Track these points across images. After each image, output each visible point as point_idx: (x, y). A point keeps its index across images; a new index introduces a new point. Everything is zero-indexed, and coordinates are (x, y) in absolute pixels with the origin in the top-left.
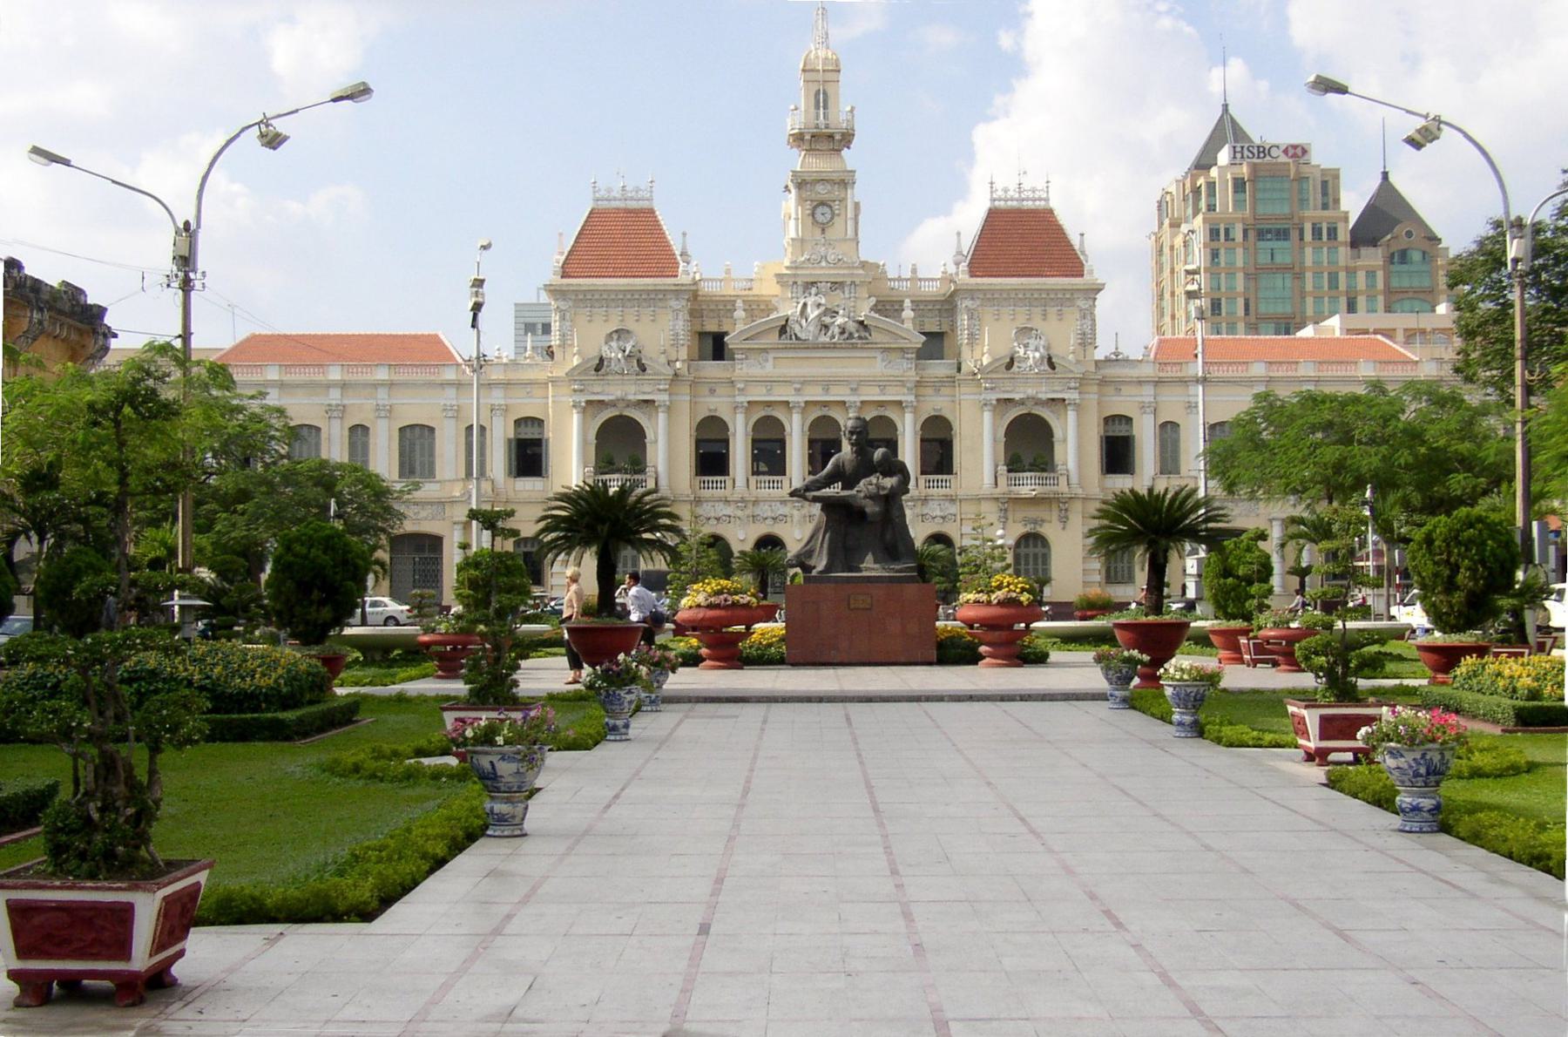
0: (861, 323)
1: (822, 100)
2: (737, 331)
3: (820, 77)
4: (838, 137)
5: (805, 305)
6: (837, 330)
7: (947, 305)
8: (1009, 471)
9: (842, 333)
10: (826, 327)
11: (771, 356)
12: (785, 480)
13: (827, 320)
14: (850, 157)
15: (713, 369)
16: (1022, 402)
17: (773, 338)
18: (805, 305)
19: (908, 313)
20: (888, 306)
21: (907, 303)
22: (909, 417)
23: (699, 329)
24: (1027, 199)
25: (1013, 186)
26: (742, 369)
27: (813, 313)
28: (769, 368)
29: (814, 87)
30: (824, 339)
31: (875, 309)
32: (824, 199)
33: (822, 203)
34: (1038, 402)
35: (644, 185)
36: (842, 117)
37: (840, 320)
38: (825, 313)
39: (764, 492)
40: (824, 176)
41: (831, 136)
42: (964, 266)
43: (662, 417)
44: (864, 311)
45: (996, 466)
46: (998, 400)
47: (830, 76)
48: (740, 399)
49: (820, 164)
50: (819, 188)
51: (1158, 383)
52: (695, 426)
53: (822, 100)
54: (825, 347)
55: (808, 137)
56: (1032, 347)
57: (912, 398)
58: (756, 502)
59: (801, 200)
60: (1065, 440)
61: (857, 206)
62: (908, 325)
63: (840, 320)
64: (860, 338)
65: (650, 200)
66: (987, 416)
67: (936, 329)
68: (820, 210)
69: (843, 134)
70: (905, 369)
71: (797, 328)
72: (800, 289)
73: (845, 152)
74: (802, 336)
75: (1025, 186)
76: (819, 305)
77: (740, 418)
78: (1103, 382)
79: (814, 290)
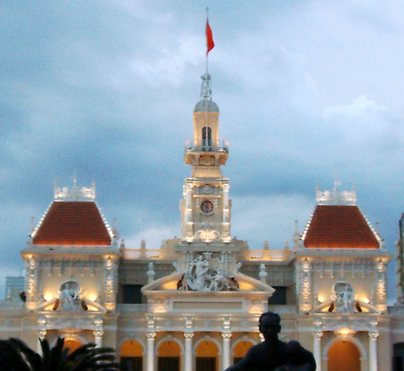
0: (233, 279)
5: (195, 267)
7: (290, 266)
13: (209, 277)
18: (195, 267)
23: (123, 283)
27: (200, 272)
38: (209, 272)
54: (207, 295)
56: (345, 297)
60: (368, 360)
63: (218, 277)
67: (282, 284)
72: (192, 257)
73: (222, 167)
76: (204, 267)
79: (201, 257)
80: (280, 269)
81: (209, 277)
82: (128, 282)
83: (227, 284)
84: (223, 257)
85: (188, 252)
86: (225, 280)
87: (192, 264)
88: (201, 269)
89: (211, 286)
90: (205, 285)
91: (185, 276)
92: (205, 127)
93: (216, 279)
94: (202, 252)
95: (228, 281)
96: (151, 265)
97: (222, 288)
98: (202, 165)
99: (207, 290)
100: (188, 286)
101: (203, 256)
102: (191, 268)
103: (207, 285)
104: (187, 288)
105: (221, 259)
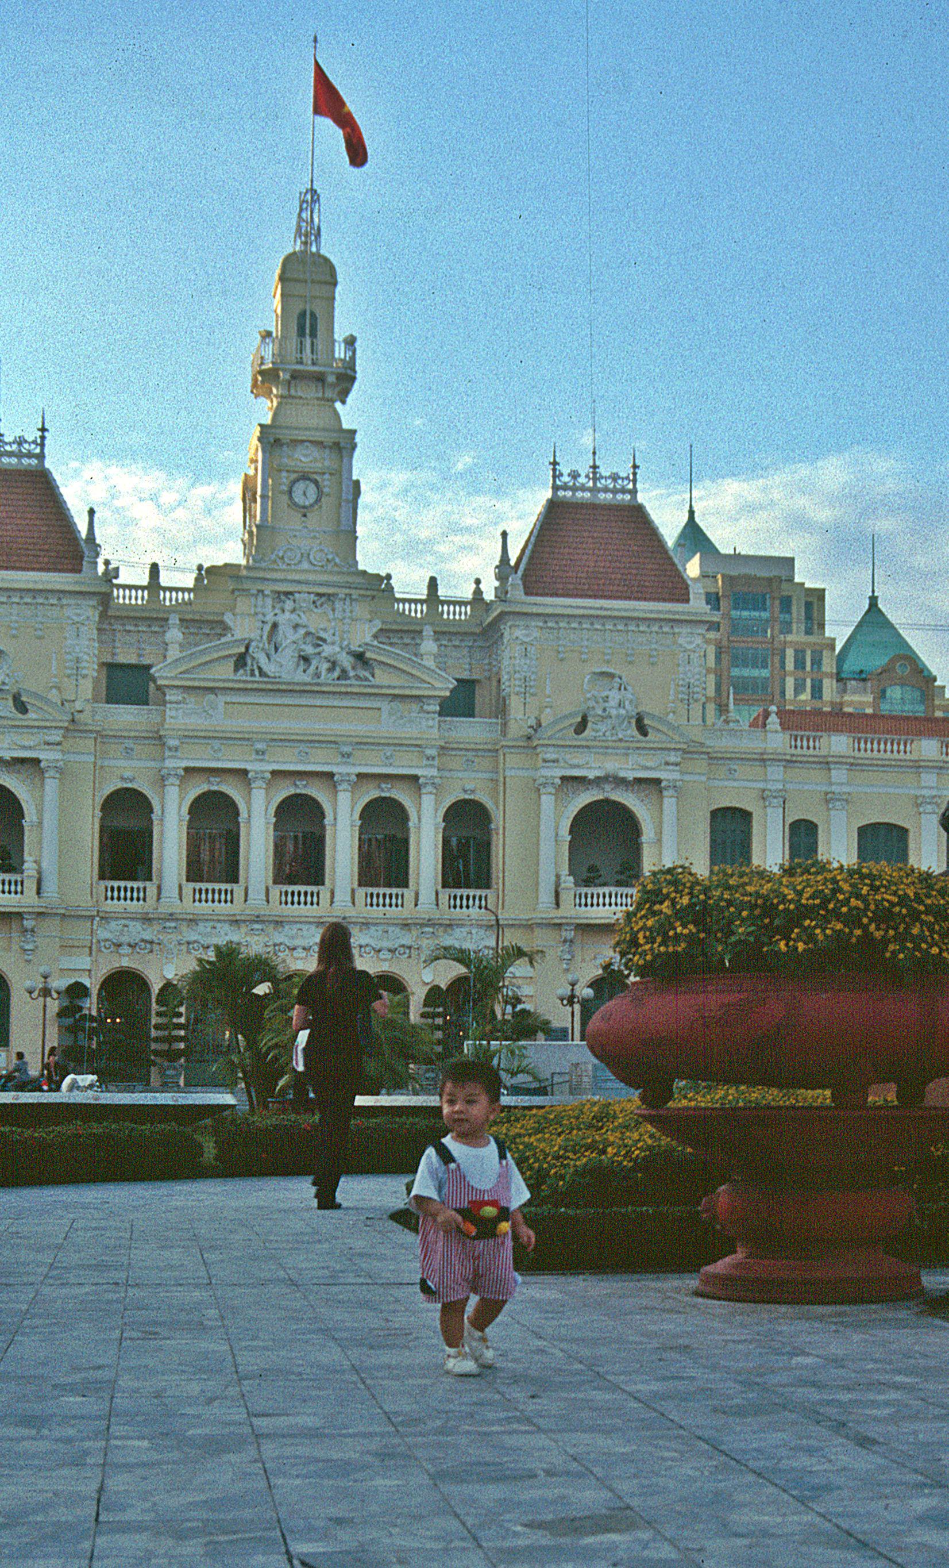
2: (170, 658)
4: (331, 379)
5: (275, 626)
6: (326, 666)
8: (576, 884)
9: (331, 670)
10: (306, 659)
11: (222, 699)
12: (238, 889)
13: (309, 650)
14: (349, 413)
15: (126, 716)
16: (598, 781)
17: (225, 671)
18: (275, 626)
20: (401, 632)
22: (428, 801)
24: (606, 490)
25: (584, 470)
26: (180, 716)
27: (287, 636)
28: (220, 715)
29: (297, 307)
30: (307, 678)
32: (306, 473)
33: (305, 477)
34: (620, 782)
35: (32, 435)
36: (340, 352)
37: (327, 650)
39: (204, 908)
41: (320, 378)
42: (515, 580)
43: (51, 786)
44: (362, 635)
45: (558, 876)
46: (563, 778)
48: (170, 763)
49: (307, 418)
51: (789, 763)
52: (99, 801)
57: (434, 772)
58: (193, 921)
61: (357, 483)
63: (327, 650)
64: (358, 677)
65: (41, 457)
66: (547, 801)
67: (465, 675)
68: (301, 486)
70: (426, 727)
71: (263, 660)
72: (269, 601)
74: (269, 668)
75: (604, 471)
76: (296, 627)
77: (172, 792)
78: (713, 759)
79: (289, 605)
82: (121, 659)
83: (349, 668)
84: (338, 605)
87: (270, 618)
89: (312, 669)
90: (298, 665)
91: (253, 644)
92: (305, 312)
93: (324, 654)
94: (291, 593)
95: (351, 659)
96: (174, 619)
97: (336, 674)
98: (293, 397)
99: (301, 677)
100: (260, 668)
101: (294, 601)
102: (267, 628)
103: (302, 665)
104: (257, 672)
105: (334, 610)
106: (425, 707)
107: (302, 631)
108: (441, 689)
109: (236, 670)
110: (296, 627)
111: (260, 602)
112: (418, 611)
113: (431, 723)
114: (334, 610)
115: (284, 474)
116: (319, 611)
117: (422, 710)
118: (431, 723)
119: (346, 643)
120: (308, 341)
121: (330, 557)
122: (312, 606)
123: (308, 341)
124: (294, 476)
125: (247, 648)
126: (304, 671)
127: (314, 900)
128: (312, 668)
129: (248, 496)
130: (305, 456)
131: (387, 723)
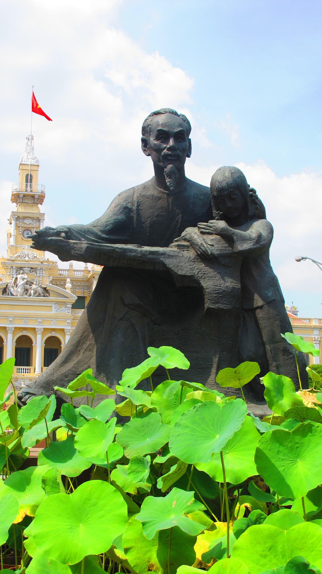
0: (45, 289)
1: (29, 179)
3: (29, 168)
4: (36, 197)
5: (16, 278)
6: (32, 292)
10: (27, 290)
13: (28, 286)
14: (42, 208)
19: (69, 285)
21: (68, 280)
27: (20, 282)
29: (26, 173)
31: (51, 282)
40: (29, 215)
41: (33, 197)
47: (35, 168)
50: (26, 221)
53: (29, 179)
55: (21, 196)
59: (17, 227)
62: (68, 291)
63: (34, 286)
64: (44, 296)
67: (82, 295)
68: (26, 232)
69: (39, 196)
71: (12, 289)
72: (15, 271)
76: (23, 279)
79: (21, 272)
80: (81, 283)
81: (28, 286)
84: (38, 272)
85: (12, 267)
86: (39, 288)
87: (15, 276)
88: (21, 280)
94: (22, 268)
97: (37, 294)
98: (25, 203)
100: (11, 293)
102: (14, 279)
103: (25, 293)
105: (36, 273)
106: (67, 306)
107: (25, 280)
108: (72, 300)
109: (3, 294)
110: (23, 279)
111: (12, 271)
112: (65, 273)
113: (69, 311)
114: (36, 273)
115: (21, 228)
116: (31, 273)
117: (66, 307)
118: (69, 311)
119: (40, 284)
120: (29, 184)
121: (35, 255)
122: (29, 272)
123: (29, 184)
124: (23, 229)
125: (7, 286)
126: (26, 294)
127: (29, 371)
128: (29, 292)
129: (9, 236)
130: (28, 222)
131: (53, 311)
